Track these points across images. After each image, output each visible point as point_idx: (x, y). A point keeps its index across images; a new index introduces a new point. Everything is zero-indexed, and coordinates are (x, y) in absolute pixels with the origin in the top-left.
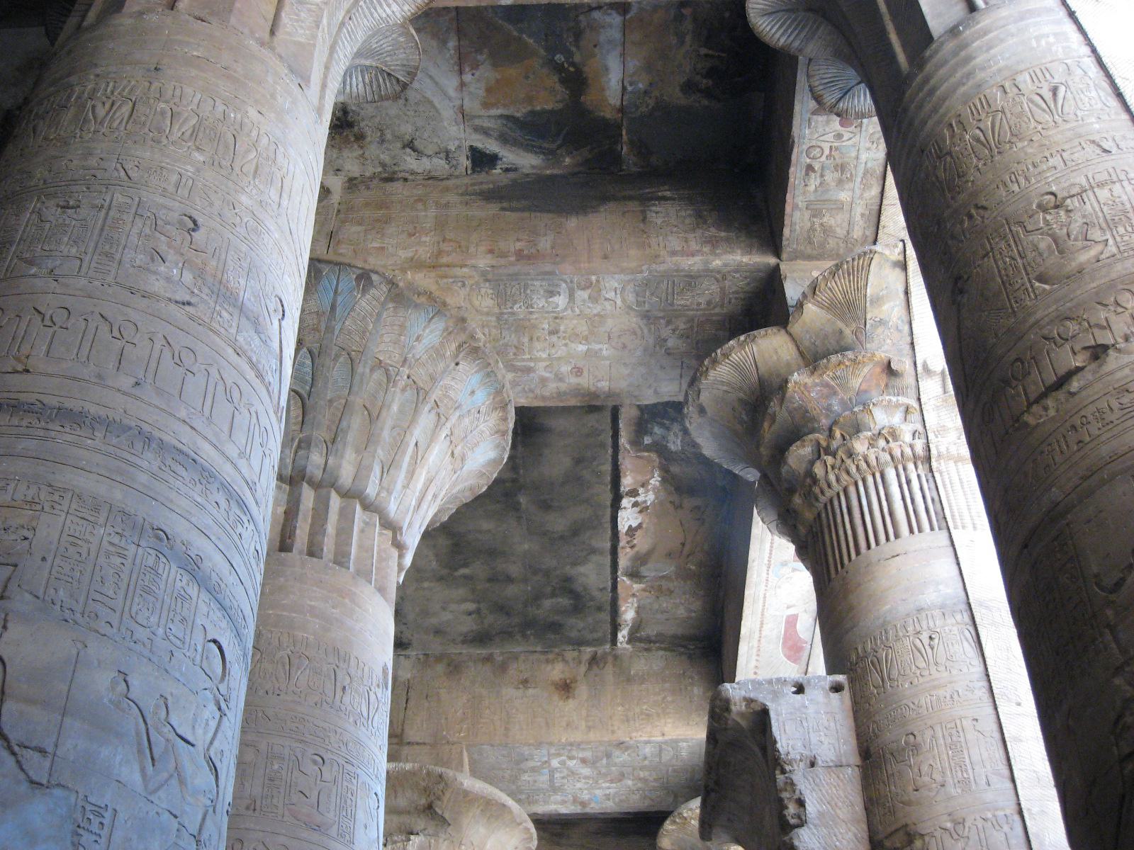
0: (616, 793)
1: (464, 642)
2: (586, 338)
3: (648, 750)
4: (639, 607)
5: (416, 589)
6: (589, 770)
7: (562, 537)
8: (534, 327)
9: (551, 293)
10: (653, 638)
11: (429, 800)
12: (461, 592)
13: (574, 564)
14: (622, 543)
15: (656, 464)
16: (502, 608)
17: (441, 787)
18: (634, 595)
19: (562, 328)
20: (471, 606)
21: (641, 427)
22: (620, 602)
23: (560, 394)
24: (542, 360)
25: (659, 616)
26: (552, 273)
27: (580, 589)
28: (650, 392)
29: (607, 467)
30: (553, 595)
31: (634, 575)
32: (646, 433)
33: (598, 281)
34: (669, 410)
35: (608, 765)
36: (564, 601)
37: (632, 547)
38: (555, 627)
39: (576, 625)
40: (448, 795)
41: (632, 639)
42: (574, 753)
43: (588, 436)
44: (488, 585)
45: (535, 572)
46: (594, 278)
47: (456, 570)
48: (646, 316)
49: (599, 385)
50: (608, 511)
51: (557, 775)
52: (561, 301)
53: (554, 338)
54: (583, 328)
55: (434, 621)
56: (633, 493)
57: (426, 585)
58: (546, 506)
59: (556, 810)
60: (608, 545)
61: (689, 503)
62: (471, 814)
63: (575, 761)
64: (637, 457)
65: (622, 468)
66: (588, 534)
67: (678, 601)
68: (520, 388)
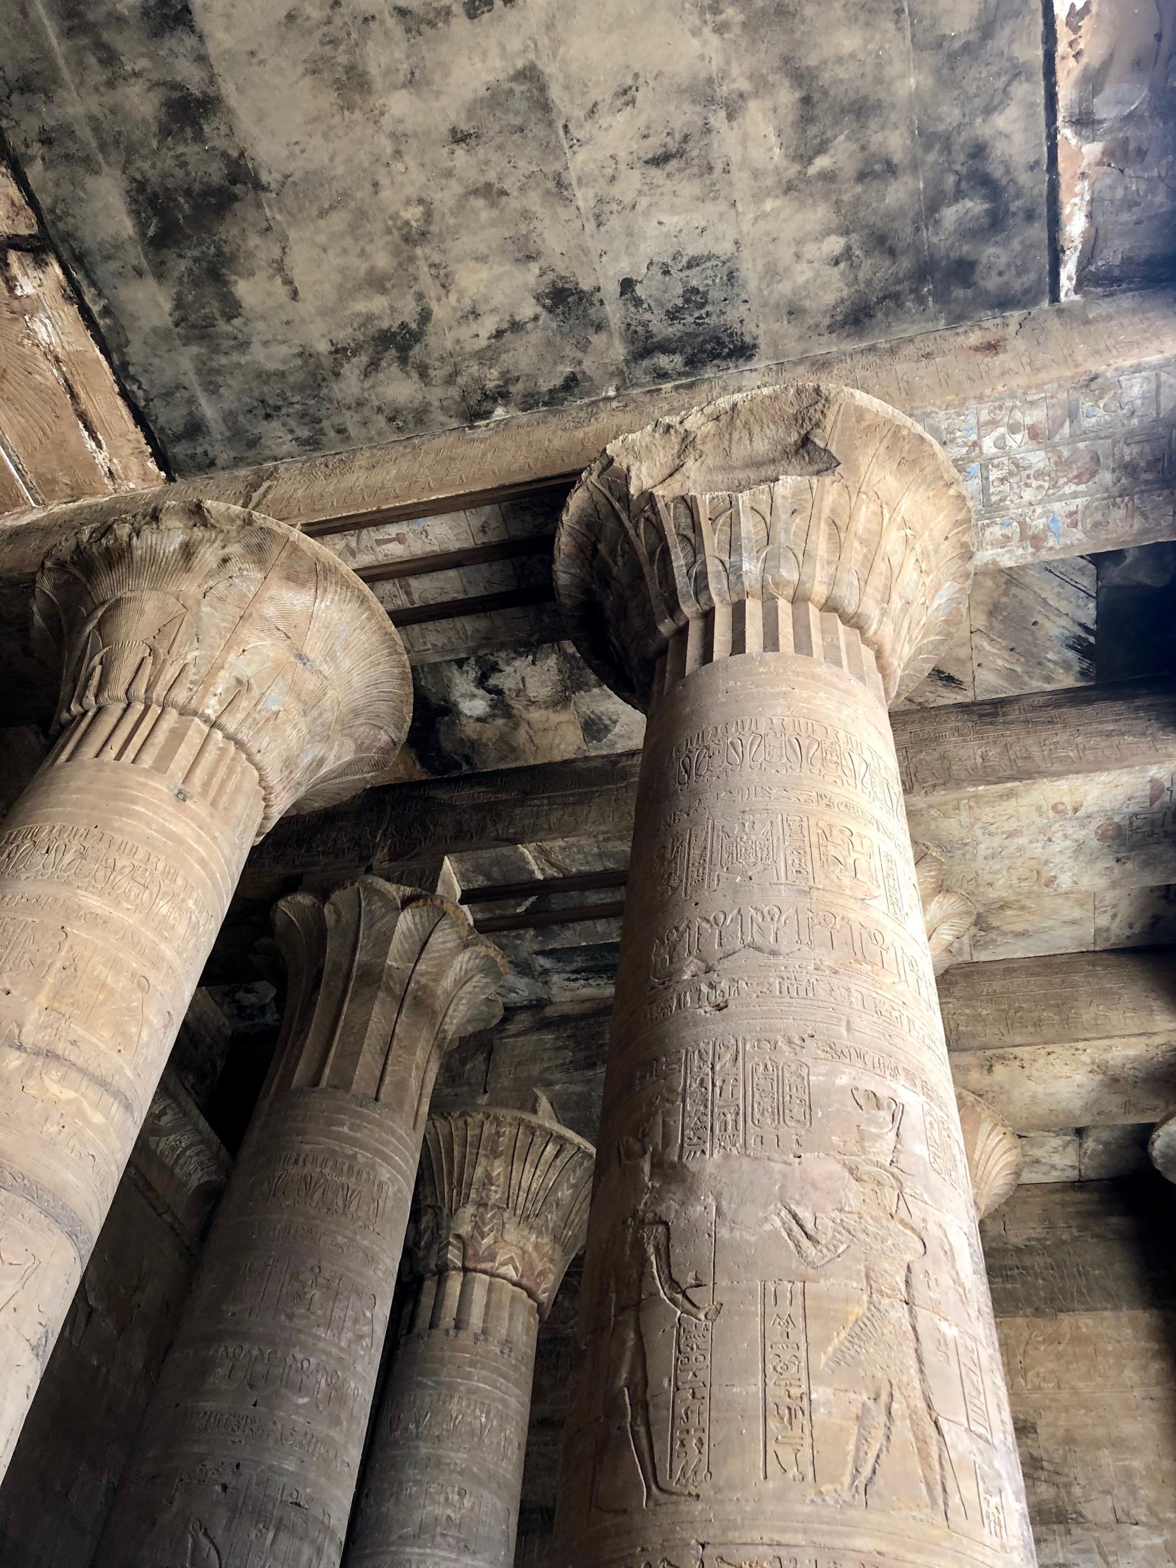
0: (1087, 507)
1: (831, 329)
3: (1136, 389)
4: (1092, 201)
5: (756, 219)
6: (1042, 454)
7: (967, 48)
10: (1117, 272)
11: (803, 432)
12: (819, 214)
13: (989, 110)
14: (1062, 48)
16: (881, 242)
17: (819, 406)
20: (835, 244)
22: (1063, 195)
25: (1125, 217)
27: (997, 172)
31: (1084, 122)
35: (1074, 438)
36: (975, 206)
37: (1078, 55)
38: (963, 270)
39: (994, 255)
40: (831, 417)
41: (1083, 281)
42: (1018, 415)
44: (859, 189)
45: (928, 148)
47: (810, 161)
51: (994, 475)
55: (785, 288)
57: (769, 205)
59: (994, 562)
60: (1040, 53)
62: (871, 452)
63: (1018, 437)
66: (1007, 31)
67: (1155, 173)
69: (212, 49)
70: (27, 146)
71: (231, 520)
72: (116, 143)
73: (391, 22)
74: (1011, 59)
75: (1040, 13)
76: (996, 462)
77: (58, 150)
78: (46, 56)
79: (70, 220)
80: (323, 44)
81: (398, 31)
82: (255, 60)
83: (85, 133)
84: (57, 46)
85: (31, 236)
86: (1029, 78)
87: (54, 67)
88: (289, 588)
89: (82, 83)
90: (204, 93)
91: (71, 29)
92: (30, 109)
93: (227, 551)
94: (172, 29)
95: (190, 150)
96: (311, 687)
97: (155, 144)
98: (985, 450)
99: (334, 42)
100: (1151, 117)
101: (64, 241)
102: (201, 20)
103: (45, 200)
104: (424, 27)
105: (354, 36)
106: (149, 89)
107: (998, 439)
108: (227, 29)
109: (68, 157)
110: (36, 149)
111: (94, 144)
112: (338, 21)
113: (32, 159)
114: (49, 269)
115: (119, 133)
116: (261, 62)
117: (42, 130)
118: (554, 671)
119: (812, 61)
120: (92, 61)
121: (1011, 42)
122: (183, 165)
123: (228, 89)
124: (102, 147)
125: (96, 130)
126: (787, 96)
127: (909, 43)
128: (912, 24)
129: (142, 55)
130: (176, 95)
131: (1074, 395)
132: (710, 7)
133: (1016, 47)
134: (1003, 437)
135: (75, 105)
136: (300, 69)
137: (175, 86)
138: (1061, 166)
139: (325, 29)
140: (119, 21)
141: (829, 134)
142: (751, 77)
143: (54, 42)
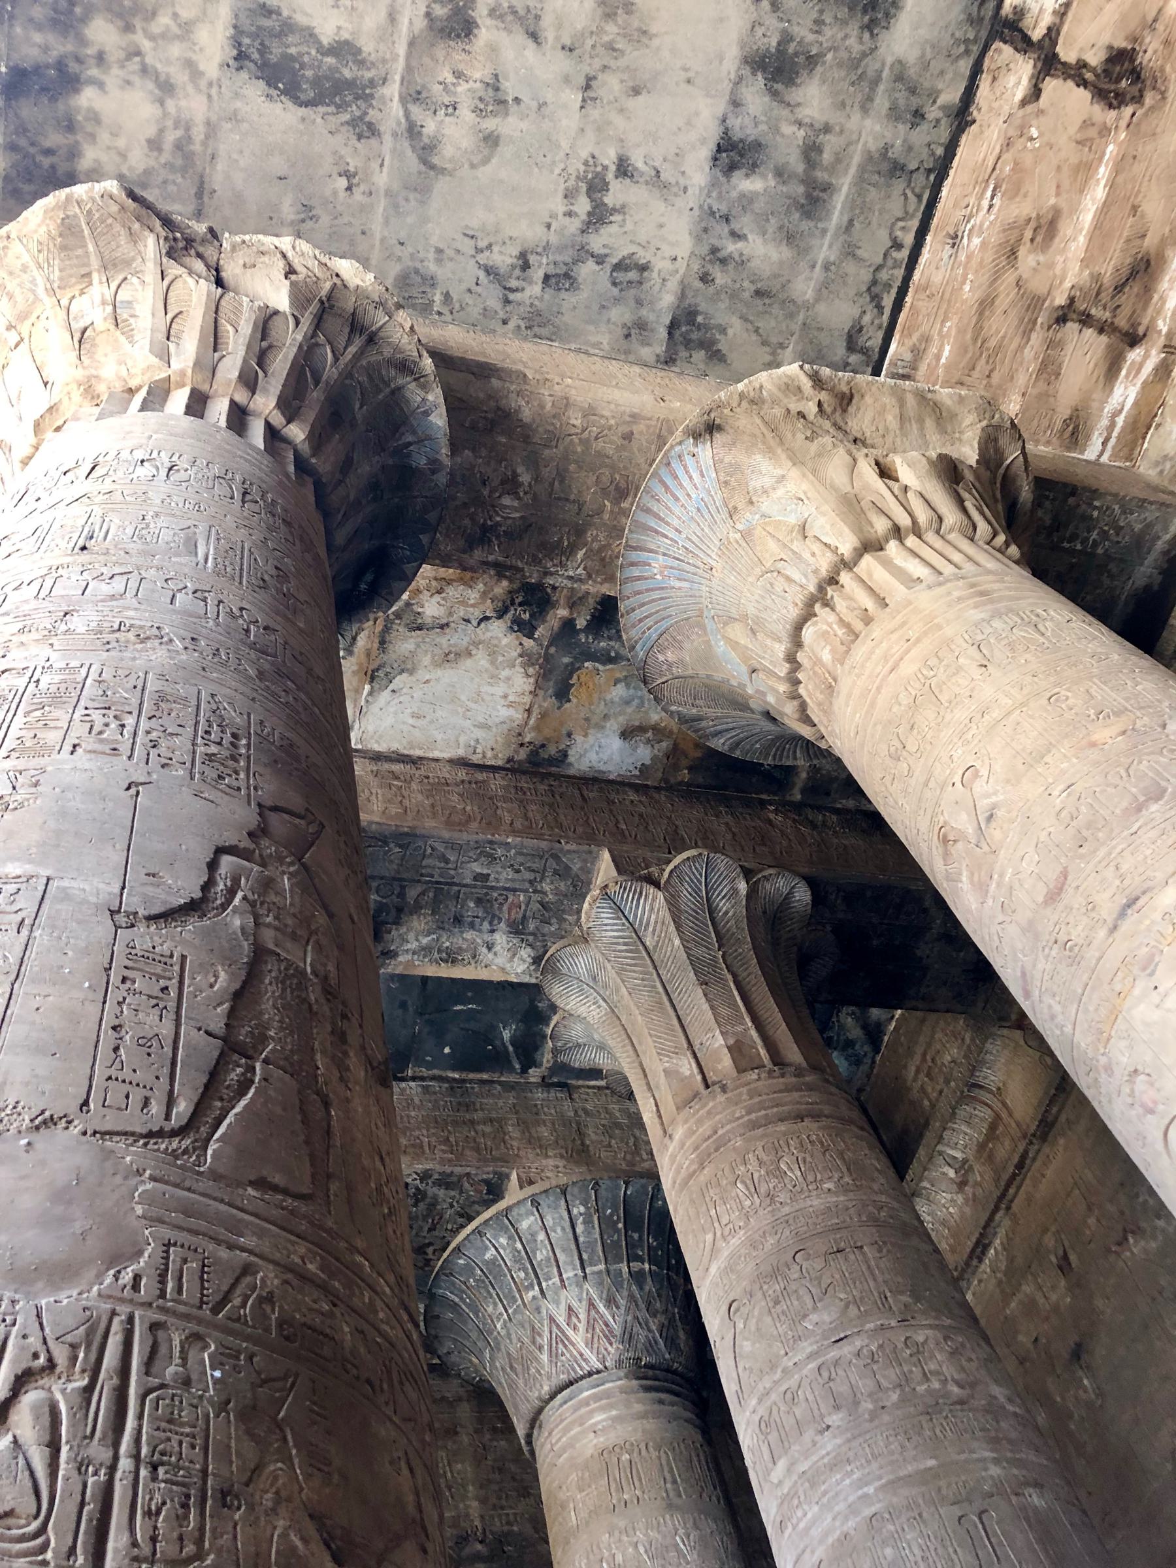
69: (721, 106)
70: (938, 121)
72: (861, 77)
73: (549, 35)
77: (915, 102)
78: (861, 181)
79: (958, 34)
80: (622, 52)
81: (547, 22)
82: (691, 74)
83: (881, 102)
84: (845, 185)
85: (1005, 42)
87: (862, 169)
89: (849, 144)
90: (754, 74)
91: (824, 190)
92: (910, 149)
94: (741, 141)
95: (802, 31)
97: (829, 56)
99: (611, 47)
101: (981, 20)
102: (713, 135)
103: (965, 66)
104: (522, 12)
105: (589, 42)
106: (799, 105)
108: (697, 114)
109: (913, 91)
110: (933, 113)
111: (881, 87)
112: (597, 63)
113: (942, 108)
115: (853, 84)
116: (686, 70)
117: (914, 125)
120: (827, 157)
122: (819, 22)
123: (731, 63)
124: (876, 81)
125: (870, 99)
129: (783, 136)
130: (779, 86)
135: (871, 131)
136: (656, 42)
137: (774, 94)
139: (613, 63)
140: (779, 173)
143: (845, 189)
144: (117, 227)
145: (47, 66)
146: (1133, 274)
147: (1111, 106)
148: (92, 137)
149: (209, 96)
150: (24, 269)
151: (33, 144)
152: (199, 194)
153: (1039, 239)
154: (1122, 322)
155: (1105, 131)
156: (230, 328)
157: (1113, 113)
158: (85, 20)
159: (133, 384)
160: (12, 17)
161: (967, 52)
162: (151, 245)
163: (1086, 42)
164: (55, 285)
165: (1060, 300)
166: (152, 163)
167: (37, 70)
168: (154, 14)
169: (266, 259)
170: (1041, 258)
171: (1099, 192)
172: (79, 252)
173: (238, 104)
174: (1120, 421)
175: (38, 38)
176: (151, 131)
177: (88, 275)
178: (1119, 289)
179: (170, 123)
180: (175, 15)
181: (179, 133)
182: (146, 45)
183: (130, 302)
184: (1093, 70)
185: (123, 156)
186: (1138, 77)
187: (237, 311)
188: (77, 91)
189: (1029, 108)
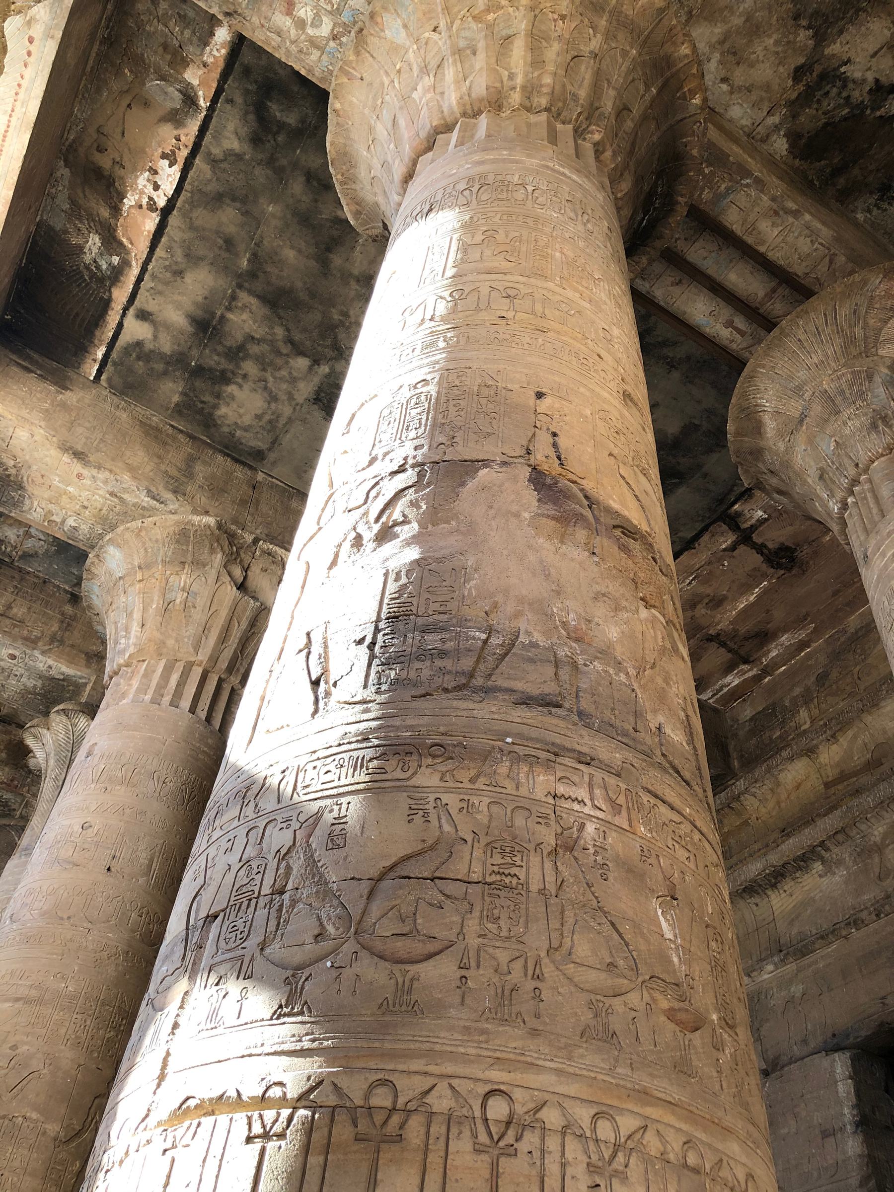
2: (65, 493)
4: (206, 44)
7: (234, 200)
8: (94, 516)
9: (75, 528)
13: (239, 157)
15: (121, 220)
18: (205, 65)
19: (78, 507)
21: (117, 274)
23: (99, 467)
24: (101, 496)
26: (68, 538)
28: (36, 438)
29: (159, 252)
30: (282, 126)
32: (114, 267)
33: (44, 521)
34: (87, 278)
36: (275, 109)
42: (293, 32)
43: (160, 293)
46: (46, 524)
48: (21, 487)
49: (69, 461)
50: (178, 204)
52: (71, 522)
53: (86, 503)
54: (64, 499)
56: (152, 205)
58: (229, 243)
60: (197, 161)
61: (104, 161)
64: (132, 243)
65: (148, 244)
66: (209, 188)
68: (124, 486)
71: (746, 472)
74: (214, 172)
75: (188, 180)
76: (329, 8)
86: (209, 154)
88: (766, 433)
93: (766, 471)
96: (820, 408)
98: (330, 27)
100: (150, 67)
103: (699, 526)
107: (317, 27)
114: (740, 509)
118: (846, 37)
119: (313, 263)
121: (210, 181)
126: (337, 260)
127: (262, 227)
128: (255, 234)
131: (247, 13)
132: (343, 326)
133: (209, 176)
134: (313, 25)
138: (215, 85)
141: (328, 224)
142: (348, 284)
144: (207, 542)
145: (217, 370)
146: (757, 635)
147: (772, 567)
148: (228, 404)
149: (294, 409)
150: (157, 541)
151: (196, 397)
152: (273, 443)
153: (711, 604)
154: (742, 652)
155: (764, 576)
156: (237, 624)
157: (772, 570)
158: (243, 359)
159: (179, 656)
160: (206, 345)
161: (703, 521)
162: (218, 558)
163: (773, 537)
164: (168, 560)
165: (712, 632)
166: (254, 423)
167: (210, 370)
168: (279, 369)
169: (273, 567)
170: (709, 612)
171: (752, 598)
172: (184, 547)
173: (308, 416)
174: (726, 690)
175: (216, 358)
176: (259, 412)
177: (183, 563)
178: (746, 639)
179: (270, 412)
180: (290, 373)
181: (272, 417)
182: (271, 379)
183: (196, 594)
184: (769, 550)
185: (241, 416)
186: (793, 560)
187: (245, 610)
188: (227, 385)
189: (726, 553)
